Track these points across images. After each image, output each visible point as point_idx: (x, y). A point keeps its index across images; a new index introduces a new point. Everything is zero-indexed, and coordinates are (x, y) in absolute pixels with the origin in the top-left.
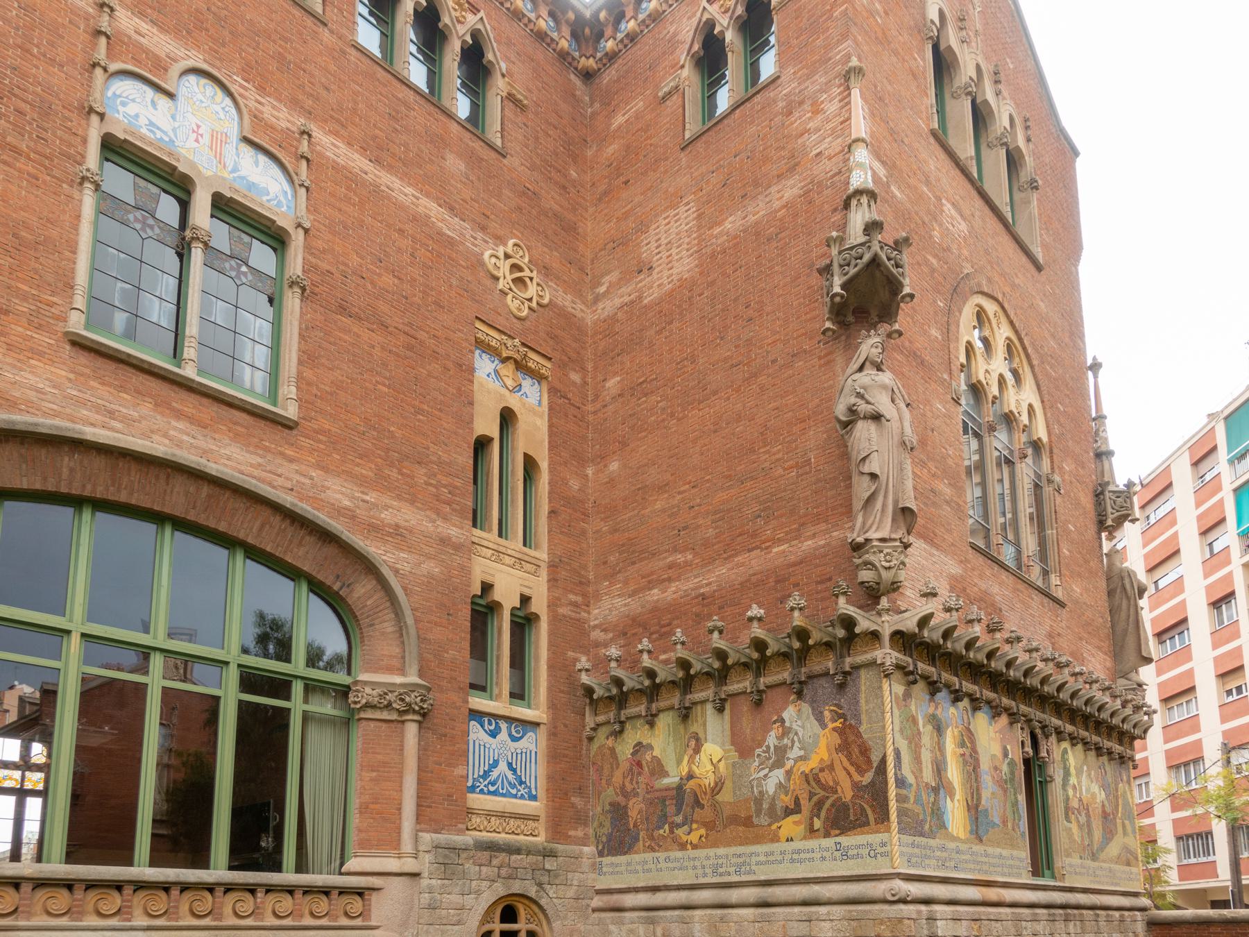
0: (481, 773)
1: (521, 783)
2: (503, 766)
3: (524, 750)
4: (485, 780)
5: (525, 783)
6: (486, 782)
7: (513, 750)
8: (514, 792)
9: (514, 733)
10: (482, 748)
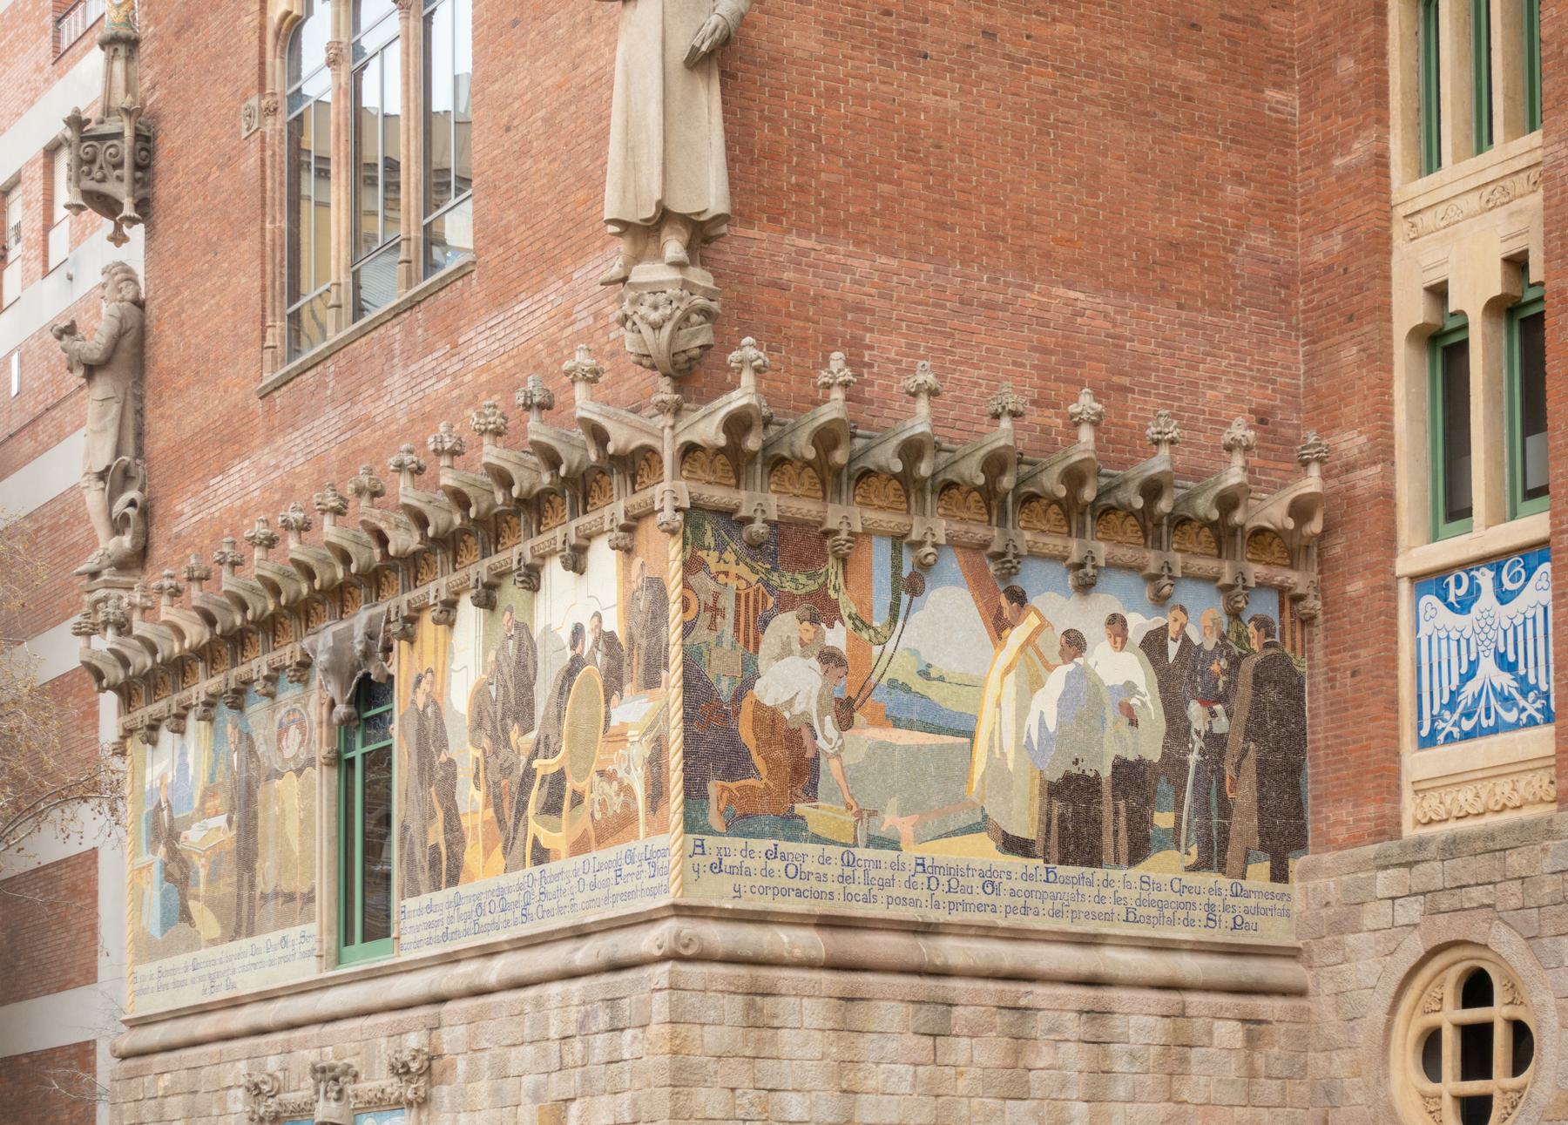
0: (1445, 700)
1: (1525, 688)
2: (1488, 668)
3: (1530, 614)
4: (1453, 712)
5: (1536, 687)
6: (1456, 716)
7: (1506, 624)
8: (1511, 717)
10: (1444, 643)
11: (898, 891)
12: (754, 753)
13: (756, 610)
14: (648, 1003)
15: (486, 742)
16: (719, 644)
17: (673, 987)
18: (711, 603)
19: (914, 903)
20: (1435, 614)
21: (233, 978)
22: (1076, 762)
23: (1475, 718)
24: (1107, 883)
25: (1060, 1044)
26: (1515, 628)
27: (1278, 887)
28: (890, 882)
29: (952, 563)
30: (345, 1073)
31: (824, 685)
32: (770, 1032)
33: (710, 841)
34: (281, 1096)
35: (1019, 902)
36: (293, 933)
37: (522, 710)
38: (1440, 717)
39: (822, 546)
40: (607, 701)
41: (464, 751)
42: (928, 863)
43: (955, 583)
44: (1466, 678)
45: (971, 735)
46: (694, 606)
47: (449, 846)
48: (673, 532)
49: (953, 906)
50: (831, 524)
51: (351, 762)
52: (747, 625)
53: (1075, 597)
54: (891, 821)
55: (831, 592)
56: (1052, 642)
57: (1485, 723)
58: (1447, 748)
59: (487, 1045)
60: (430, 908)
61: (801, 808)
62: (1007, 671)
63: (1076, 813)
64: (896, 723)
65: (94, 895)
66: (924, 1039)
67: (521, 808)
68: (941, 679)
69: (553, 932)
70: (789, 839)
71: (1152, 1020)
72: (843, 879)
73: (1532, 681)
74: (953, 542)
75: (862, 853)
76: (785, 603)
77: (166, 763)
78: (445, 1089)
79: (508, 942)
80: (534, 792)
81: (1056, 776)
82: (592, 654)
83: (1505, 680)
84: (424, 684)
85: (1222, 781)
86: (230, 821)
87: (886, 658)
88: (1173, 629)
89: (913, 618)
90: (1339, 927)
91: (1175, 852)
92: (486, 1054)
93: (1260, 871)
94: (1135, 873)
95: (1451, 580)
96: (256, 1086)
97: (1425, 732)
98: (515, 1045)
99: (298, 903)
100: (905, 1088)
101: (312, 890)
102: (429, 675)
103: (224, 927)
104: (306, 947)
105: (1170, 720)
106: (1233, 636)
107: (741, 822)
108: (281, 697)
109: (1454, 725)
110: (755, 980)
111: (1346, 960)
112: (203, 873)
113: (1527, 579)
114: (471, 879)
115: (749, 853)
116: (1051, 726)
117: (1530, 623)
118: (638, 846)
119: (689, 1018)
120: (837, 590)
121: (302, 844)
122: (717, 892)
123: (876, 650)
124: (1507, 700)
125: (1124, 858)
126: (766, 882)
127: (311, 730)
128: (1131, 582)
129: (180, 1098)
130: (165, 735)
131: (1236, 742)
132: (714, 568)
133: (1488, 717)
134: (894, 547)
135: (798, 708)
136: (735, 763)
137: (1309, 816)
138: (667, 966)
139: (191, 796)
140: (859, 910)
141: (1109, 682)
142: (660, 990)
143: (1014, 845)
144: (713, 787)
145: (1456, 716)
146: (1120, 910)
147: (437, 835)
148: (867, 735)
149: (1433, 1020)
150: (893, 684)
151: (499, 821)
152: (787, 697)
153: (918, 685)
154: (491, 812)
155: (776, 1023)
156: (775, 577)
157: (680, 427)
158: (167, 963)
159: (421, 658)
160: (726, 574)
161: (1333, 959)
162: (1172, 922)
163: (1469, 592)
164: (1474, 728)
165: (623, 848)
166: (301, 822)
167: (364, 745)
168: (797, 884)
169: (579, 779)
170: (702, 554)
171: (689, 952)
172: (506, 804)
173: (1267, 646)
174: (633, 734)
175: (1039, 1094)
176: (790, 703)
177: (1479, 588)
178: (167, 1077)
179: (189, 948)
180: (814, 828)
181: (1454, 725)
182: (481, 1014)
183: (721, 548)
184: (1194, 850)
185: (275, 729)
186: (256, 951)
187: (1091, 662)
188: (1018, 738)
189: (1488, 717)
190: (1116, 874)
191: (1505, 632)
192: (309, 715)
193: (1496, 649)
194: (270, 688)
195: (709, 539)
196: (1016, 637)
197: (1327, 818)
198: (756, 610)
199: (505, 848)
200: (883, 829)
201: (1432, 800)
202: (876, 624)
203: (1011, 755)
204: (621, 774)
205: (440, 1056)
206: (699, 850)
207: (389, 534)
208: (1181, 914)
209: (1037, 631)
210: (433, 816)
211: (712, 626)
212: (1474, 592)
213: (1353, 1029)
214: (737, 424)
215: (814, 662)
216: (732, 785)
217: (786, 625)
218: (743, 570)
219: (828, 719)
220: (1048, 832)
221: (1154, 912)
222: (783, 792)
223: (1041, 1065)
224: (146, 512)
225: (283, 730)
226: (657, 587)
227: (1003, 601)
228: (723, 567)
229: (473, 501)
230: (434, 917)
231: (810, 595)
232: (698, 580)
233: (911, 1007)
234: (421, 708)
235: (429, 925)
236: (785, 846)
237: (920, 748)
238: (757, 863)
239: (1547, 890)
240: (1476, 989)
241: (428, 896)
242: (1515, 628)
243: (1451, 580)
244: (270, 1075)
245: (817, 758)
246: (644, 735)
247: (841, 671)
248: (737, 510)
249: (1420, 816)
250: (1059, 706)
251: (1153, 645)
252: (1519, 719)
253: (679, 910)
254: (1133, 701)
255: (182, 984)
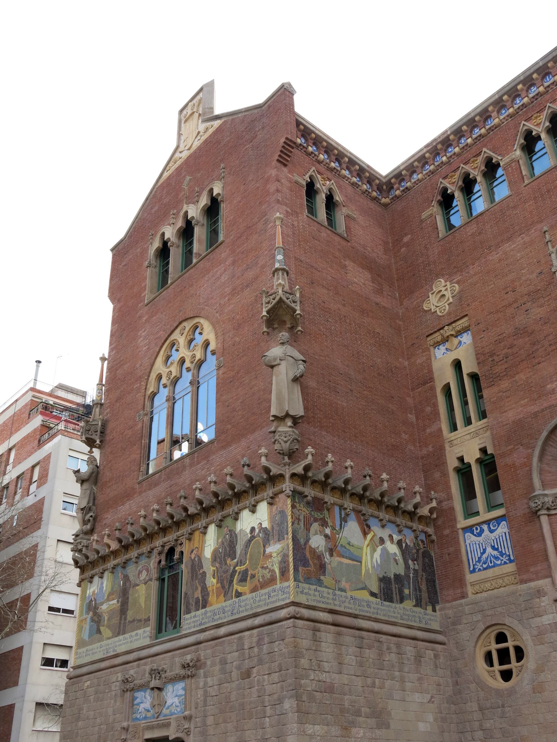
0: (477, 560)
1: (502, 554)
2: (489, 550)
3: (500, 535)
4: (480, 563)
5: (505, 553)
6: (481, 564)
7: (493, 538)
8: (499, 562)
9: (492, 528)
10: (474, 545)
11: (347, 604)
12: (310, 561)
13: (309, 521)
14: (285, 632)
15: (217, 565)
16: (300, 529)
17: (294, 626)
18: (298, 517)
19: (351, 608)
20: (470, 538)
21: (115, 648)
22: (385, 573)
23: (487, 564)
24: (395, 608)
25: (391, 654)
26: (496, 539)
27: (434, 613)
28: (345, 602)
29: (353, 515)
30: (162, 671)
31: (326, 544)
32: (319, 643)
33: (300, 584)
34: (134, 682)
35: (376, 611)
36: (140, 631)
37: (233, 555)
38: (476, 564)
39: (323, 506)
40: (264, 546)
41: (209, 568)
42: (353, 597)
43: (354, 521)
44: (482, 554)
45: (361, 562)
46: (294, 517)
47: (203, 597)
48: (288, 497)
49: (360, 610)
50: (326, 500)
51: (163, 580)
52: (307, 525)
53: (381, 529)
54: (344, 584)
55: (326, 519)
56: (377, 540)
57: (490, 565)
58: (479, 573)
59: (219, 654)
60: (195, 616)
61: (322, 577)
62: (368, 546)
63: (386, 587)
64: (343, 557)
65: (20, 660)
66: (358, 649)
67: (231, 582)
68: (353, 546)
69: (245, 617)
70: (319, 586)
71: (411, 648)
72: (333, 599)
73: (504, 552)
74: (354, 510)
75: (338, 592)
76: (316, 520)
77: (95, 587)
78: (202, 671)
79: (227, 622)
80: (236, 576)
81: (381, 576)
82: (258, 534)
83: (495, 553)
84: (194, 552)
85: (418, 582)
86: (118, 602)
87: (340, 538)
88: (403, 540)
89: (346, 528)
90: (454, 624)
91: (410, 601)
92: (219, 657)
93: (430, 608)
94: (402, 606)
95: (474, 528)
96: (127, 679)
97: (471, 569)
98: (230, 653)
99: (143, 622)
100: (354, 664)
101: (149, 617)
102: (196, 549)
103: (113, 633)
104: (145, 635)
105: (405, 564)
106: (416, 544)
107: (307, 580)
108: (140, 563)
109: (481, 566)
110: (315, 626)
111: (458, 633)
112: (106, 618)
113: (498, 526)
114: (211, 605)
115: (309, 589)
116: (379, 562)
117: (501, 537)
118: (278, 586)
119: (298, 636)
120: (327, 519)
121: (145, 604)
122: (302, 599)
123: (337, 536)
124: (497, 558)
125: (399, 601)
126: (314, 598)
127: (151, 571)
128: (393, 526)
129: (93, 688)
130: (96, 579)
131: (420, 572)
132: (298, 508)
133: (491, 563)
134: (340, 509)
135: (320, 549)
136: (305, 563)
137: (439, 594)
138: (292, 620)
139: (104, 596)
140: (337, 608)
141: (391, 552)
142: (289, 627)
143: (373, 594)
144: (300, 569)
145: (481, 564)
146: (399, 616)
147: (198, 594)
148: (337, 559)
149: (488, 648)
150: (341, 545)
151: (222, 587)
152: (317, 546)
153: (348, 547)
154: (219, 585)
155: (321, 640)
156: (313, 513)
157: (291, 469)
158: (90, 647)
159: (193, 544)
160: (301, 510)
161: (453, 633)
162: (411, 621)
163: (480, 531)
164: (487, 566)
165: (271, 588)
166: (145, 598)
167: (168, 574)
168: (322, 599)
169: (254, 570)
170: (295, 504)
171: (298, 616)
172: (225, 582)
173: (424, 547)
174: (274, 555)
175: (387, 669)
176: (318, 547)
177: (483, 530)
178: (89, 682)
179: (99, 641)
180: (325, 584)
181: (481, 566)
182: (216, 645)
183: (299, 503)
184: (414, 601)
185: (137, 572)
186: (125, 639)
187: (386, 546)
188: (372, 565)
189: (491, 563)
190: (398, 606)
191: (493, 540)
192: (150, 567)
193: (491, 545)
194: (137, 560)
195: (297, 500)
196: (369, 537)
197: (444, 595)
198: (309, 521)
199: (225, 594)
200: (342, 586)
201: (477, 587)
202: (337, 529)
203: (370, 569)
204: (270, 567)
205: (200, 661)
206: (297, 587)
207: (189, 508)
208: (413, 619)
209: (373, 536)
210: (197, 588)
211: (298, 524)
212: (482, 531)
213: (463, 653)
214: (307, 468)
215: (323, 537)
216: (305, 569)
217: (315, 526)
218: (305, 509)
219: (327, 553)
220: (381, 592)
221: (407, 617)
222: (317, 573)
223: (387, 659)
224: (95, 519)
225: (140, 572)
226: (282, 513)
227: (365, 527)
228: (301, 508)
229: (220, 495)
230: (196, 619)
231: (321, 519)
232: (294, 510)
233: (354, 638)
234: (193, 558)
235: (194, 622)
236: (319, 588)
237: (349, 564)
238: (312, 592)
239: (523, 606)
240: (501, 638)
241: (194, 613)
242: (496, 539)
243: (474, 528)
244: (132, 675)
245: (325, 564)
246: (279, 554)
247: (329, 540)
248: (303, 493)
249: (473, 592)
250: (380, 557)
251: (399, 543)
252: (501, 563)
253: (294, 604)
254: (396, 558)
255: (96, 653)
